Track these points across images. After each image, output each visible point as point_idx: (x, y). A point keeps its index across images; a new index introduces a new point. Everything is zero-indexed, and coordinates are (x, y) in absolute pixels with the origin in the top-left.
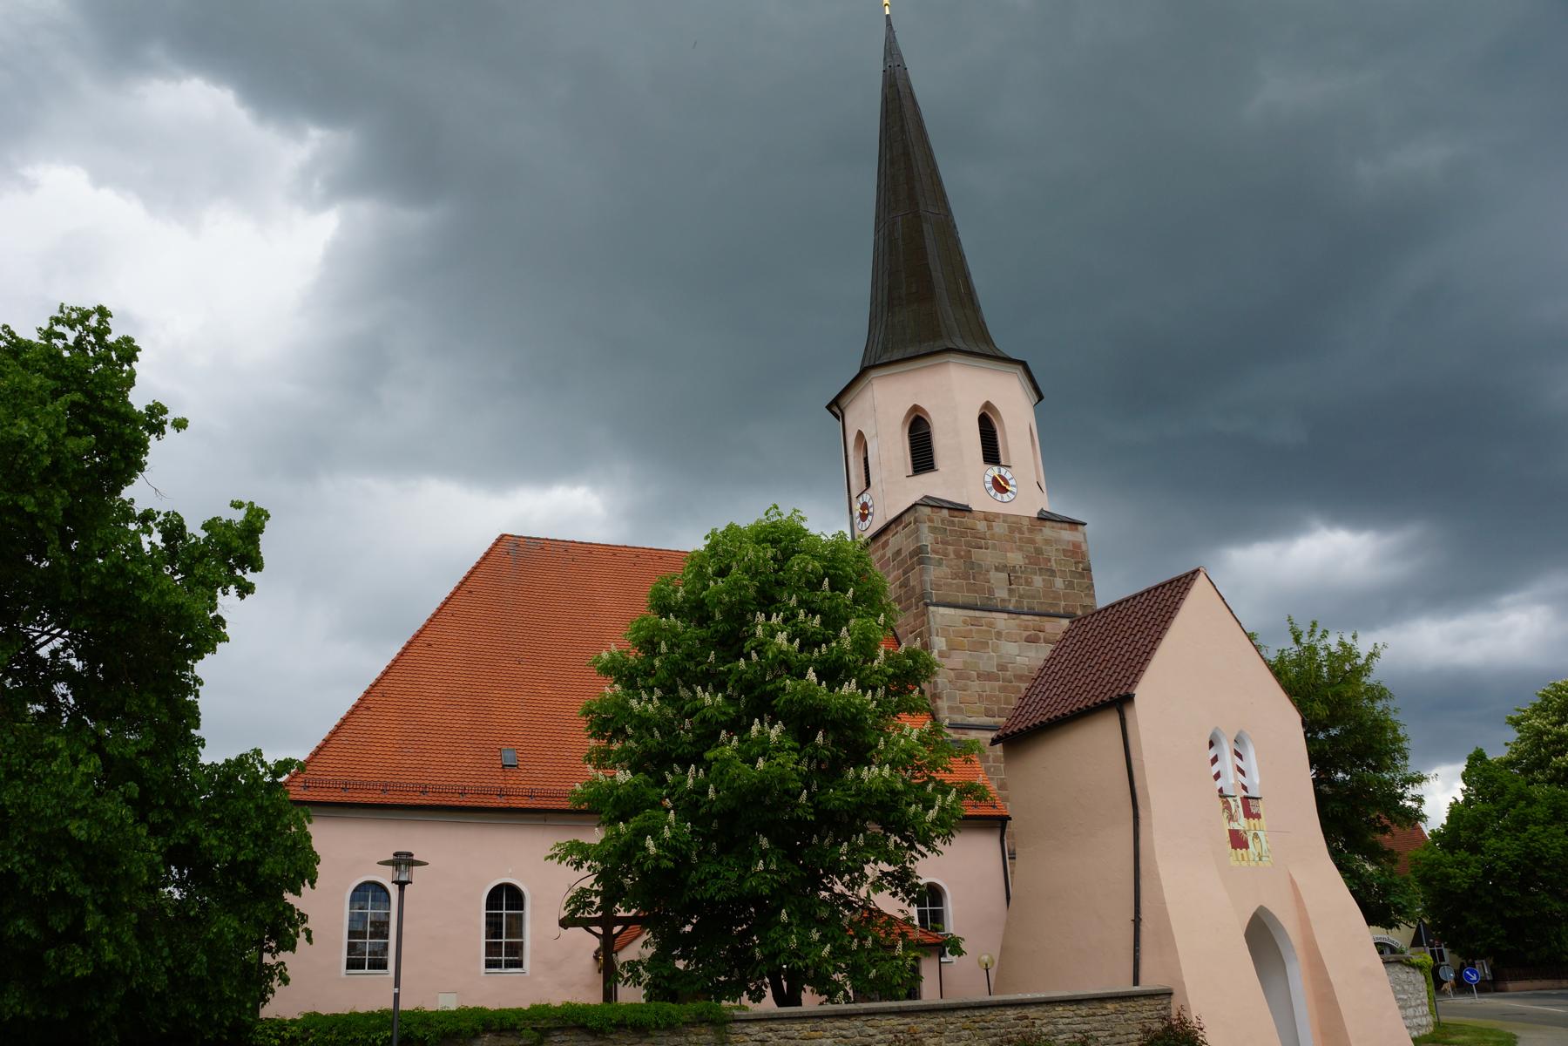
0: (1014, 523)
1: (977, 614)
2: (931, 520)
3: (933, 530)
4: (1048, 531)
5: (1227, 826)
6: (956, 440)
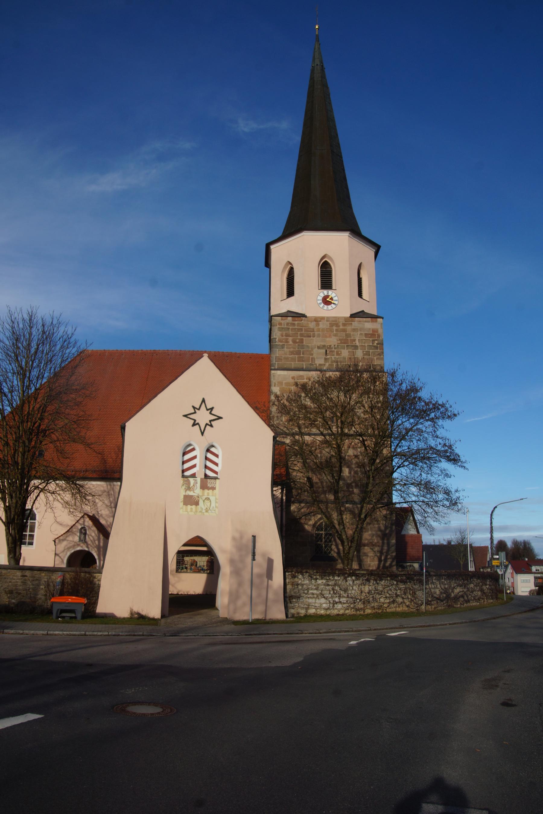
0: (334, 322)
1: (301, 373)
2: (280, 324)
3: (280, 329)
4: (356, 323)
5: (182, 493)
6: (308, 278)
